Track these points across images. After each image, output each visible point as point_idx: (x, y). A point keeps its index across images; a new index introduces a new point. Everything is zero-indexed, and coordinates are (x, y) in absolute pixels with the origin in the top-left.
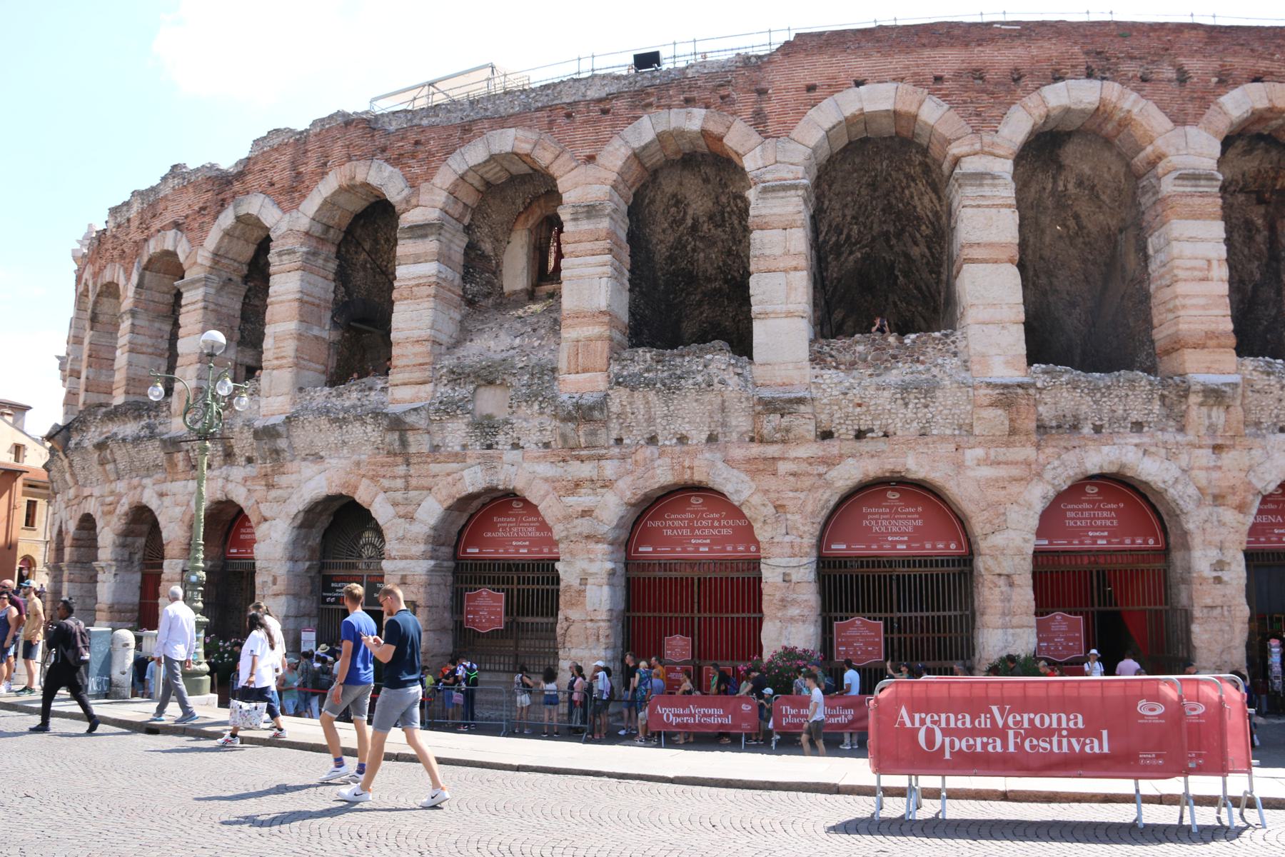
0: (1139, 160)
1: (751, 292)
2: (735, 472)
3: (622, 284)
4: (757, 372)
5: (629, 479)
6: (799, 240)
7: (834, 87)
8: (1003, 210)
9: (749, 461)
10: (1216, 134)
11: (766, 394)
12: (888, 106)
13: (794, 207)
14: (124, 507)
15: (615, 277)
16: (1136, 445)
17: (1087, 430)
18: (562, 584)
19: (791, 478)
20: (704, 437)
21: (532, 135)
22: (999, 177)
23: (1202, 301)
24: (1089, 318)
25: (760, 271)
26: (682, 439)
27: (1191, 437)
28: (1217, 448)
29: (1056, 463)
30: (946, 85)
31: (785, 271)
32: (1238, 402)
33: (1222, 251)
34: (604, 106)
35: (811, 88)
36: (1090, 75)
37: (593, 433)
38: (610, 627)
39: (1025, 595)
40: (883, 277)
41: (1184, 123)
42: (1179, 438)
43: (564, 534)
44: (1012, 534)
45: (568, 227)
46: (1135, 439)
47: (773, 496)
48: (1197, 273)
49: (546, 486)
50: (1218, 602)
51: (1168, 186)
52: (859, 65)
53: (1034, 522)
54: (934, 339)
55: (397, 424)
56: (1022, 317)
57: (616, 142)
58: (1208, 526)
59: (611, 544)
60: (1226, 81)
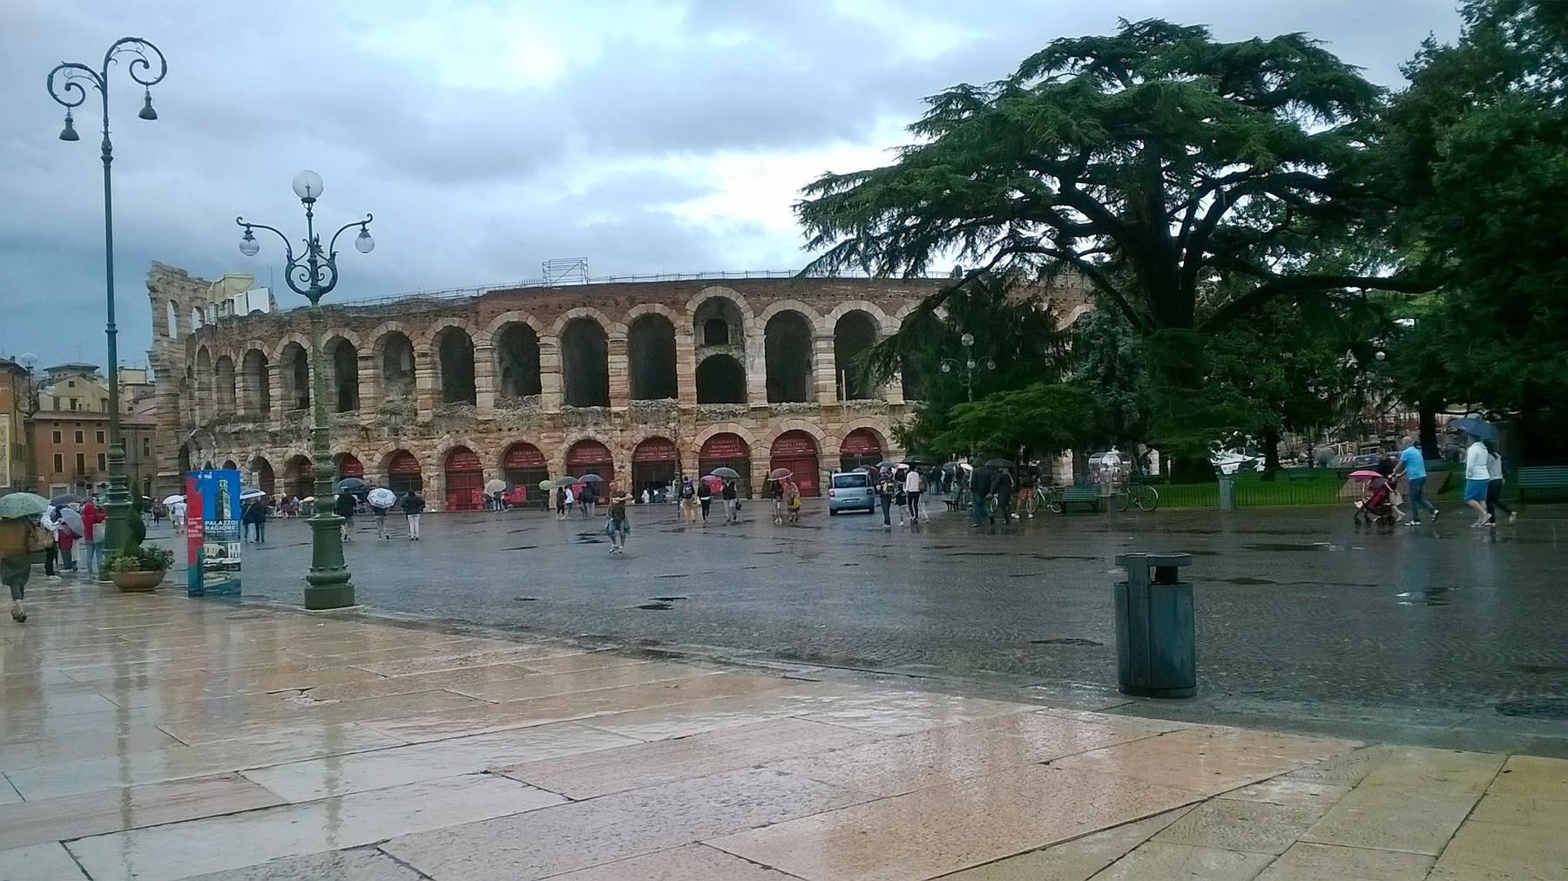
14: (251, 458)
15: (435, 376)
34: (426, 314)
40: (522, 376)
52: (508, 304)
55: (364, 428)
60: (633, 303)
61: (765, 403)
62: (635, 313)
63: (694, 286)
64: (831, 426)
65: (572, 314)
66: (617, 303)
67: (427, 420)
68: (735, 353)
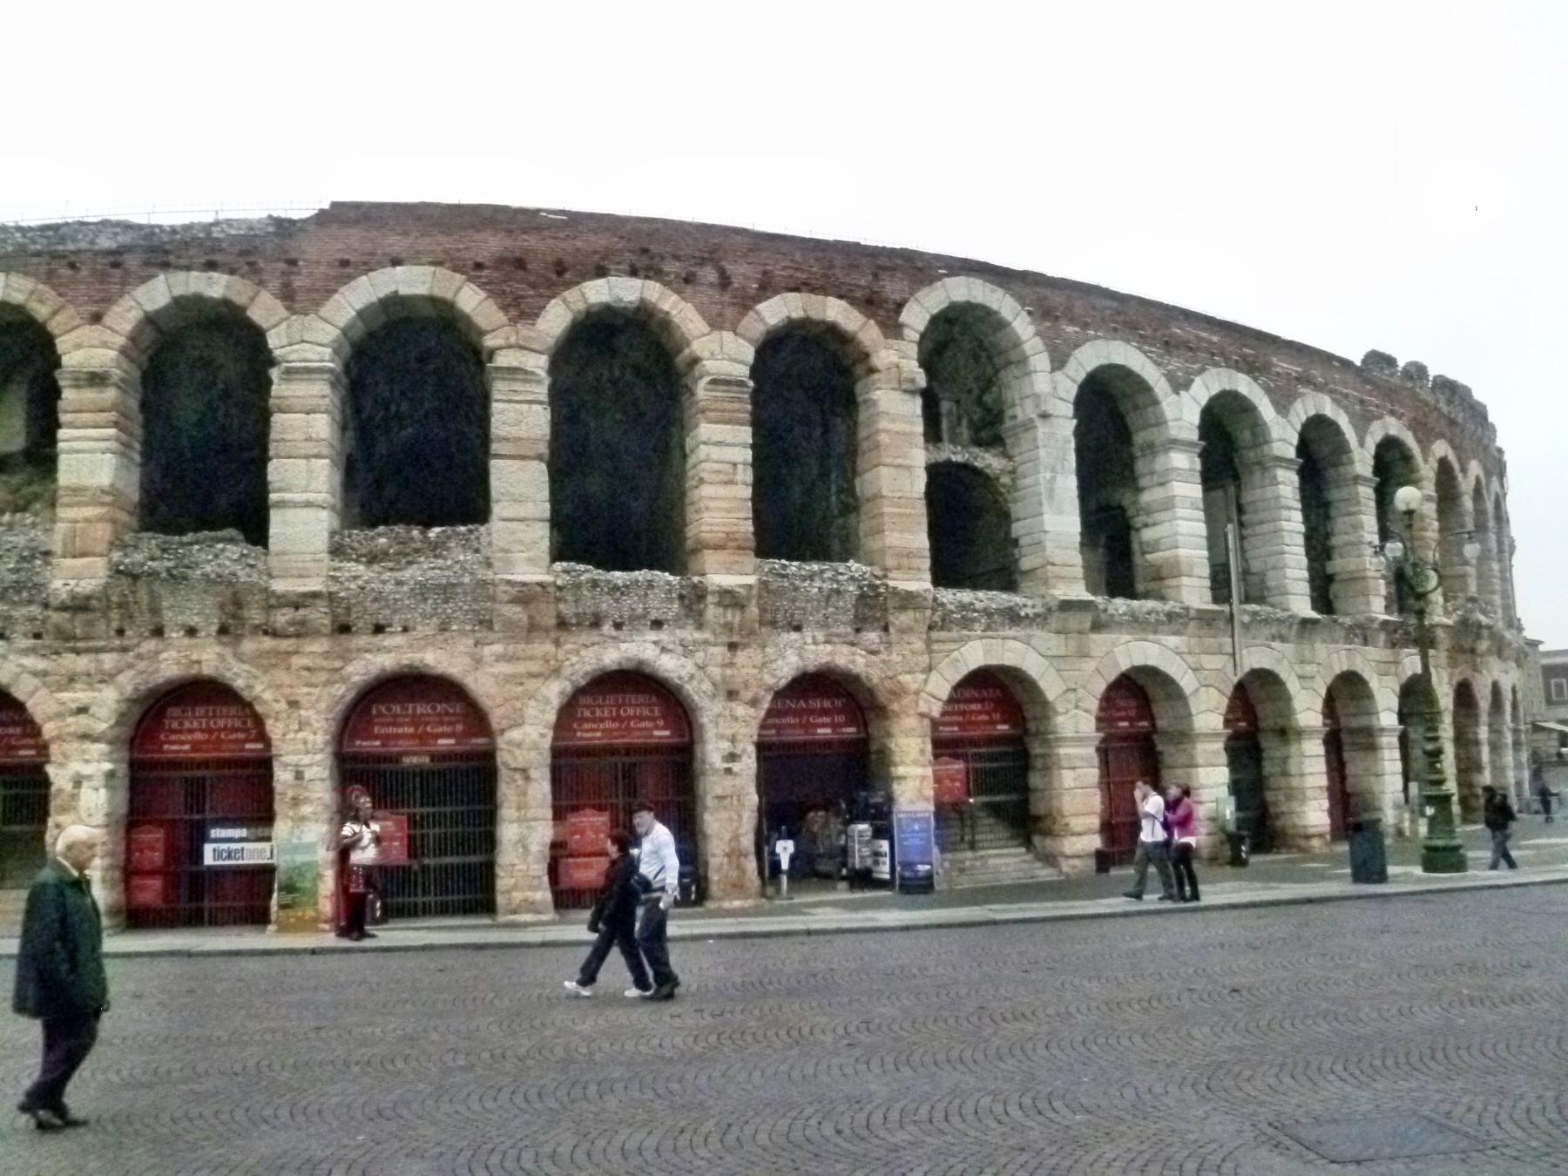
0: (680, 360)
1: (270, 478)
2: (246, 667)
3: (131, 459)
4: (273, 561)
5: (131, 673)
6: (322, 426)
7: (368, 267)
8: (535, 407)
9: (262, 654)
10: (750, 341)
11: (279, 586)
12: (422, 290)
13: (320, 391)
16: (655, 643)
17: (607, 628)
18: (53, 789)
19: (305, 673)
20: (214, 628)
21: (29, 284)
22: (532, 373)
23: (725, 505)
24: (617, 516)
25: (279, 457)
26: (191, 632)
27: (707, 635)
28: (732, 647)
29: (575, 659)
30: (485, 273)
31: (307, 457)
32: (754, 601)
33: (748, 455)
34: (115, 258)
35: (345, 263)
36: (634, 272)
37: (90, 623)
38: (109, 833)
39: (541, 788)
41: (721, 328)
42: (698, 635)
43: (55, 733)
44: (528, 729)
45: (68, 395)
46: (653, 636)
47: (287, 691)
48: (721, 477)
49: (36, 681)
50: (729, 792)
51: (702, 391)
52: (395, 243)
53: (551, 717)
54: (458, 534)
56: (547, 514)
57: (127, 302)
58: (721, 720)
59: (110, 742)
61: (1079, 592)
62: (776, 310)
63: (920, 268)
64: (1212, 662)
65: (597, 292)
66: (724, 282)
67: (87, 586)
68: (989, 461)
